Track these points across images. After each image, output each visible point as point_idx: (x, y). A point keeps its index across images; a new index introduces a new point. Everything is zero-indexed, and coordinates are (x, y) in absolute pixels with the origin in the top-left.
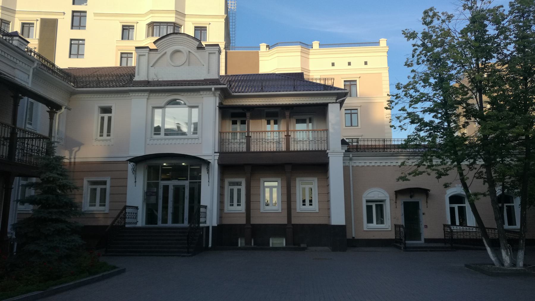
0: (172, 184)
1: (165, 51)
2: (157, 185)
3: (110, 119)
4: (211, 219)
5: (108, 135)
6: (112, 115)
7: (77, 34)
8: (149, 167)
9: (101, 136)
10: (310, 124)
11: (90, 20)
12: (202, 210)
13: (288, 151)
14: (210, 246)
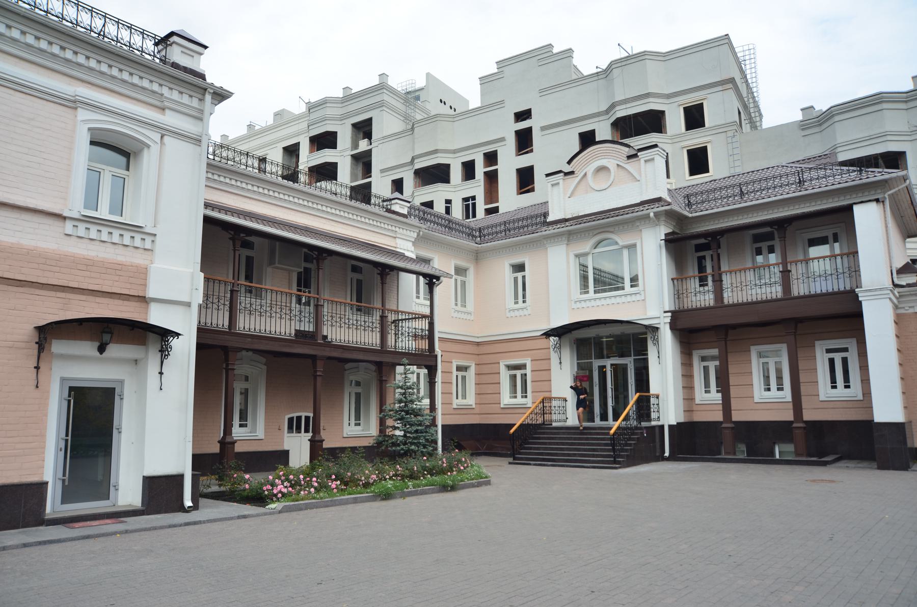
1: (583, 174)
3: (524, 277)
5: (524, 302)
9: (516, 303)
10: (837, 245)
12: (653, 400)
14: (667, 454)
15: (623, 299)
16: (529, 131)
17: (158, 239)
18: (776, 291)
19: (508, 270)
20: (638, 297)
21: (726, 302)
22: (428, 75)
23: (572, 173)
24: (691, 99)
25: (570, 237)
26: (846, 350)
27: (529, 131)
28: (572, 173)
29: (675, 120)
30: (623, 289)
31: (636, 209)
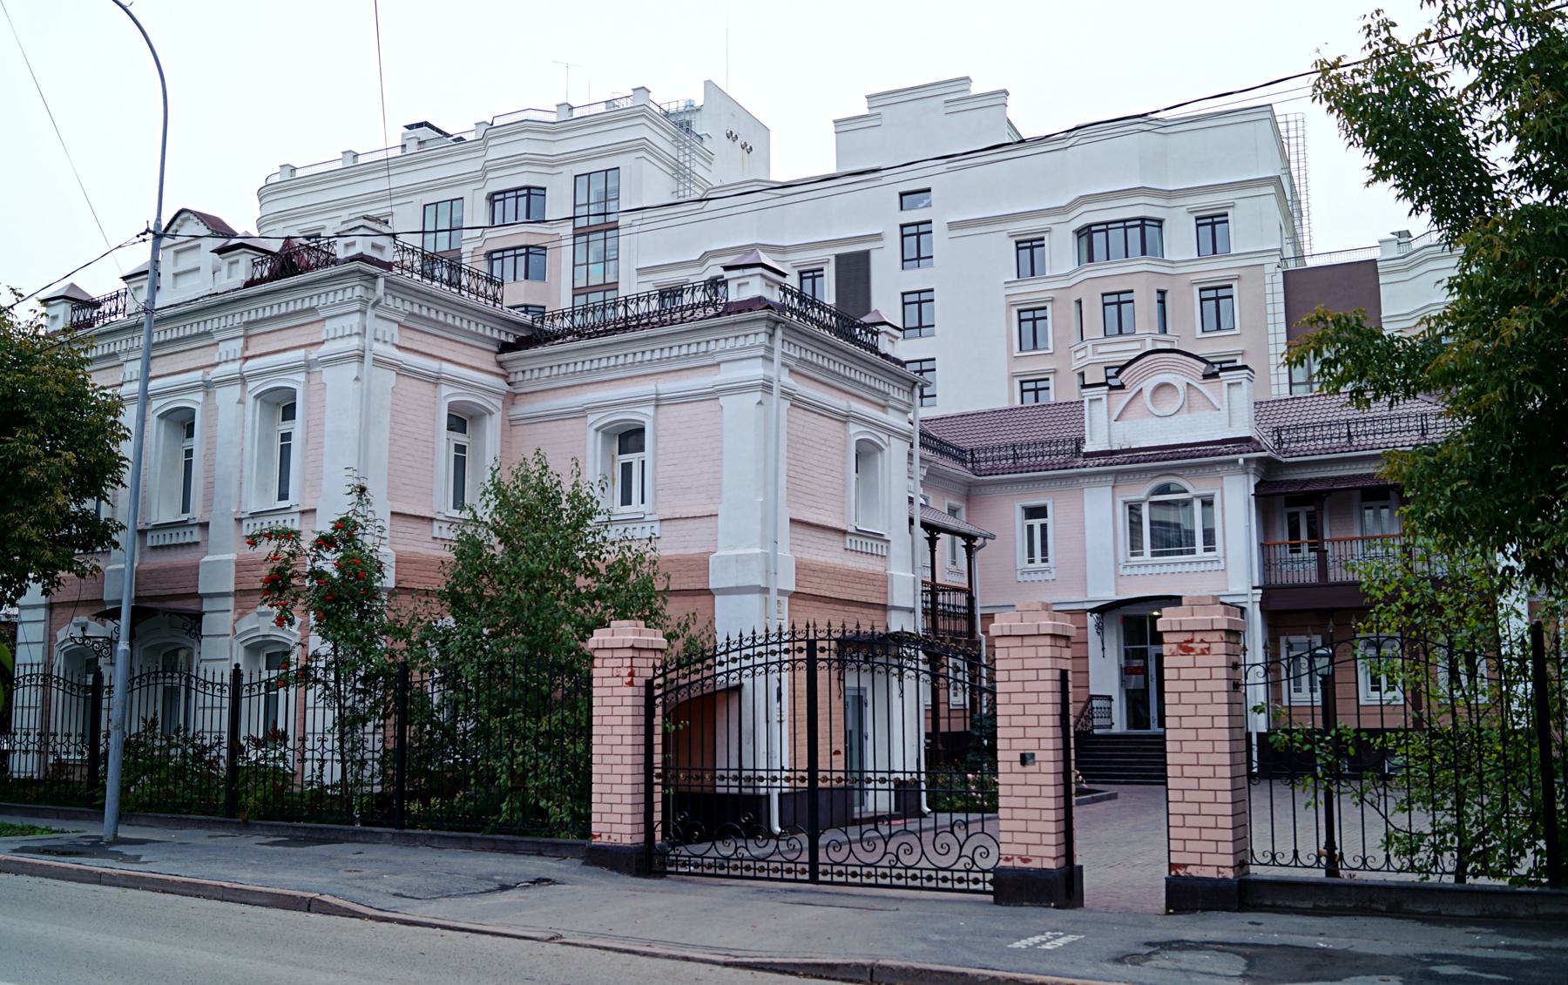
2: (1143, 654)
3: (1044, 527)
6: (1049, 521)
7: (916, 279)
8: (1126, 620)
9: (1031, 562)
11: (939, 241)
15: (1194, 567)
17: (892, 544)
19: (1019, 514)
20: (1215, 566)
21: (1331, 578)
22: (709, 84)
23: (1122, 387)
28: (1122, 387)
29: (1180, 240)
30: (1193, 552)
31: (1223, 448)
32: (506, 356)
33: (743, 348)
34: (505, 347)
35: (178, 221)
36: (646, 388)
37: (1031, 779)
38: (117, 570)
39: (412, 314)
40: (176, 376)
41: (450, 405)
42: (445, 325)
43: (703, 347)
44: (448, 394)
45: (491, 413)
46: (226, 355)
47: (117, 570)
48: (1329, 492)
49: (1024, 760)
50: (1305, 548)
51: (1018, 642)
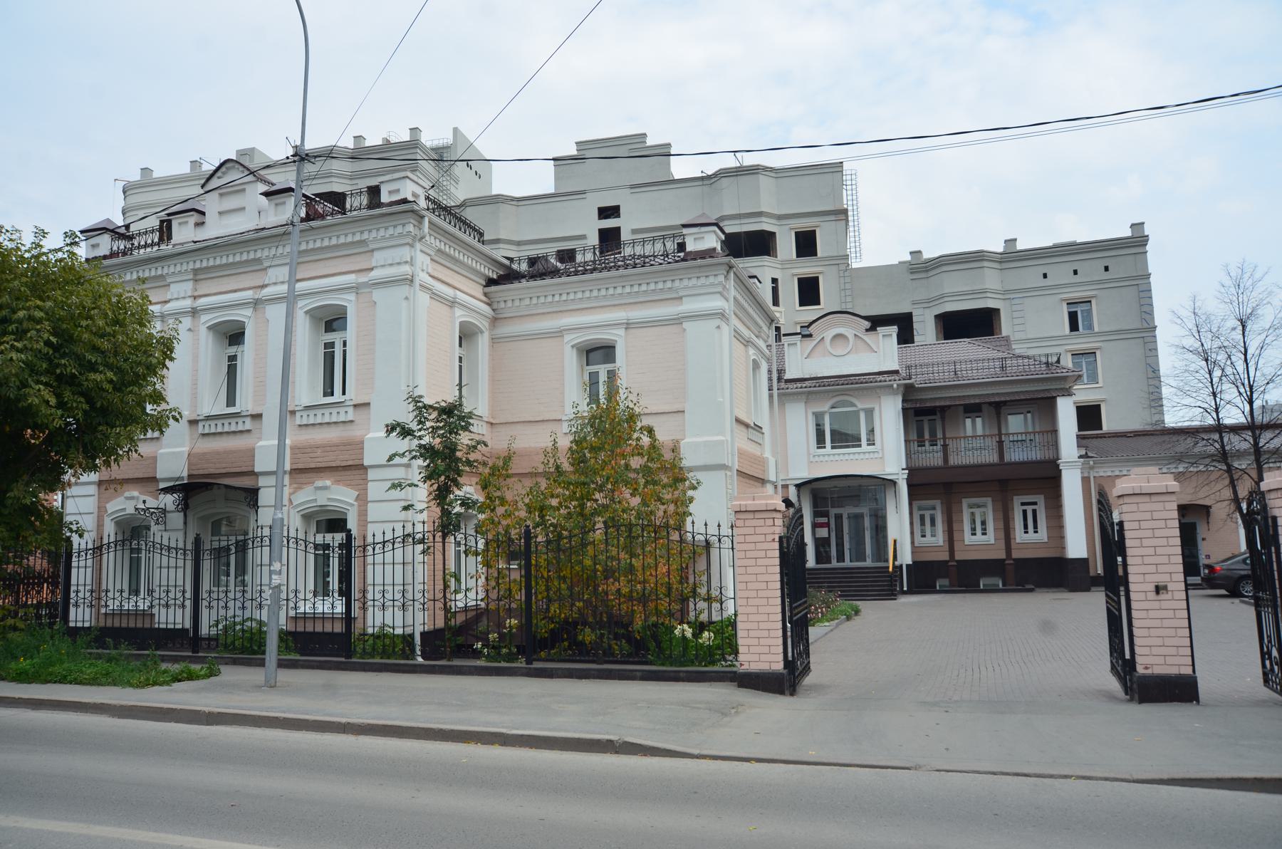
0: (846, 511)
2: (826, 515)
4: (906, 558)
13: (1002, 463)
15: (862, 456)
16: (617, 230)
18: (992, 458)
22: (456, 130)
23: (810, 336)
24: (804, 224)
25: (809, 397)
26: (1035, 503)
27: (617, 230)
29: (786, 245)
30: (860, 446)
31: (881, 378)
32: (493, 288)
33: (703, 286)
34: (490, 282)
35: (223, 169)
36: (620, 315)
37: (1165, 605)
38: (171, 453)
39: (439, 250)
40: (226, 296)
41: (461, 323)
42: (456, 261)
43: (669, 284)
44: (460, 315)
45: (482, 332)
46: (276, 280)
47: (171, 453)
48: (949, 407)
49: (1158, 589)
50: (927, 443)
51: (1147, 499)
